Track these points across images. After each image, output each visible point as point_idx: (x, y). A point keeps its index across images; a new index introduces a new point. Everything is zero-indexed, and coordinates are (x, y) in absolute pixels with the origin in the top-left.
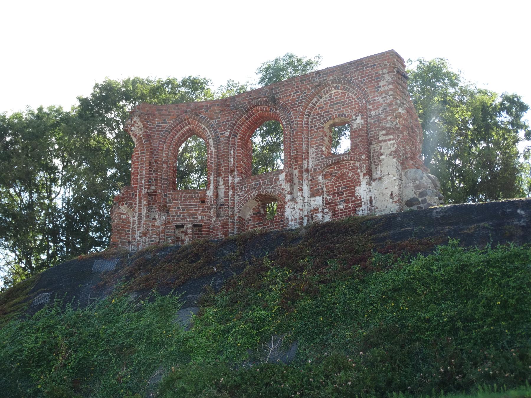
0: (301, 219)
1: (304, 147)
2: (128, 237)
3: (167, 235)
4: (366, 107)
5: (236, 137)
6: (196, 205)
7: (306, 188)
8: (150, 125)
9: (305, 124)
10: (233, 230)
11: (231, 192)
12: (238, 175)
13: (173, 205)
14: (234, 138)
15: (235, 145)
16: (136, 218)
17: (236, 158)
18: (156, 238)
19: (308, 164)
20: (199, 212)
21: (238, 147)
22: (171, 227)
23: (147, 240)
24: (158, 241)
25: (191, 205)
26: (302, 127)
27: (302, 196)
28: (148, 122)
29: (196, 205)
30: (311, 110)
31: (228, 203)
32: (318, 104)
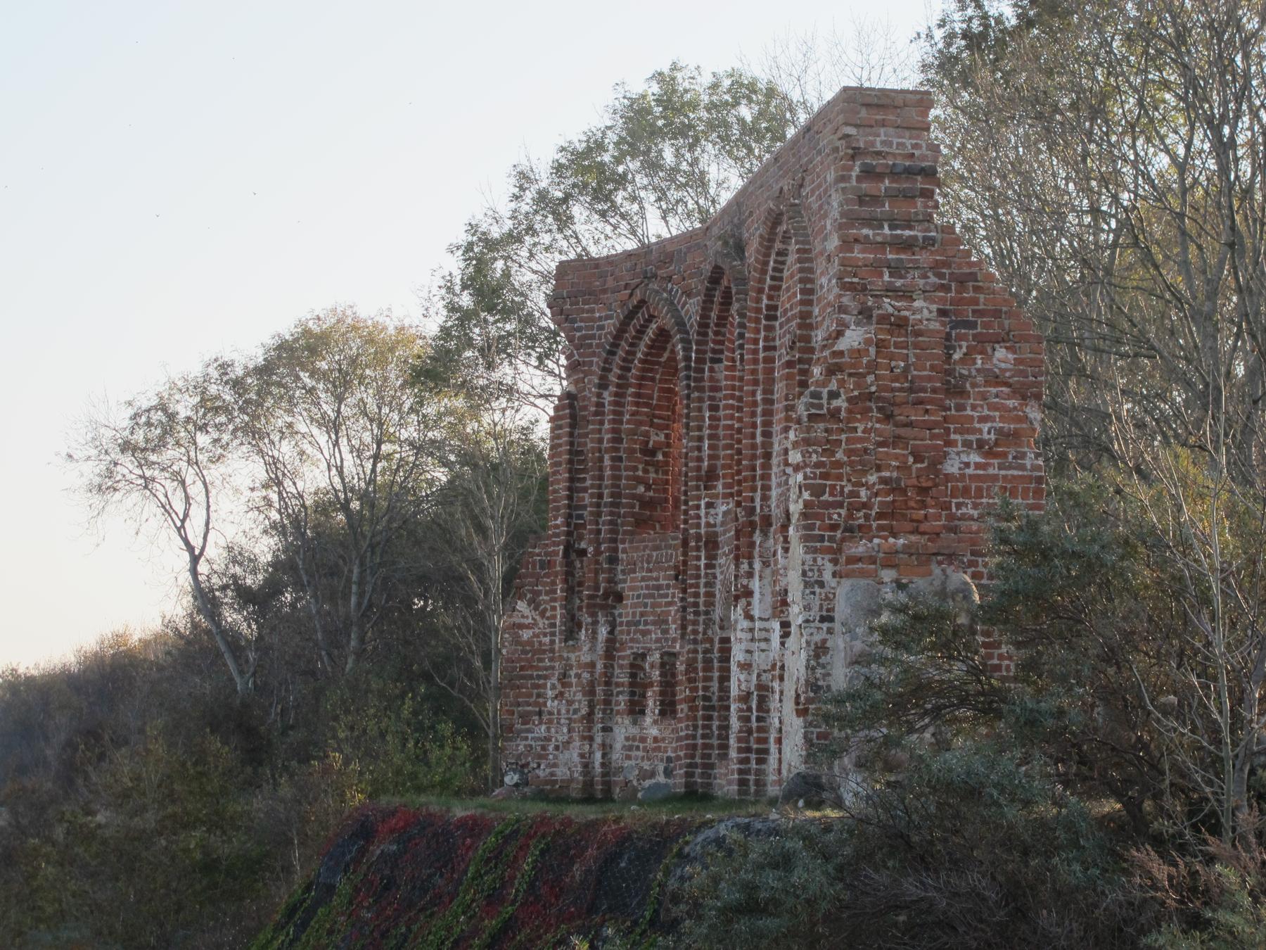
0: (745, 698)
1: (759, 439)
2: (539, 696)
3: (618, 685)
4: (809, 314)
5: (719, 361)
6: (668, 586)
7: (755, 585)
8: (579, 329)
9: (766, 349)
10: (706, 689)
11: (703, 562)
12: (726, 496)
13: (632, 589)
14: (712, 370)
15: (715, 389)
16: (547, 640)
17: (721, 432)
18: (580, 702)
19: (765, 498)
20: (673, 609)
21: (726, 397)
22: (623, 658)
23: (563, 711)
24: (583, 712)
25: (659, 588)
26: (756, 361)
27: (750, 617)
28: (573, 321)
29: (668, 586)
30: (770, 298)
31: (697, 595)
32: (786, 274)
